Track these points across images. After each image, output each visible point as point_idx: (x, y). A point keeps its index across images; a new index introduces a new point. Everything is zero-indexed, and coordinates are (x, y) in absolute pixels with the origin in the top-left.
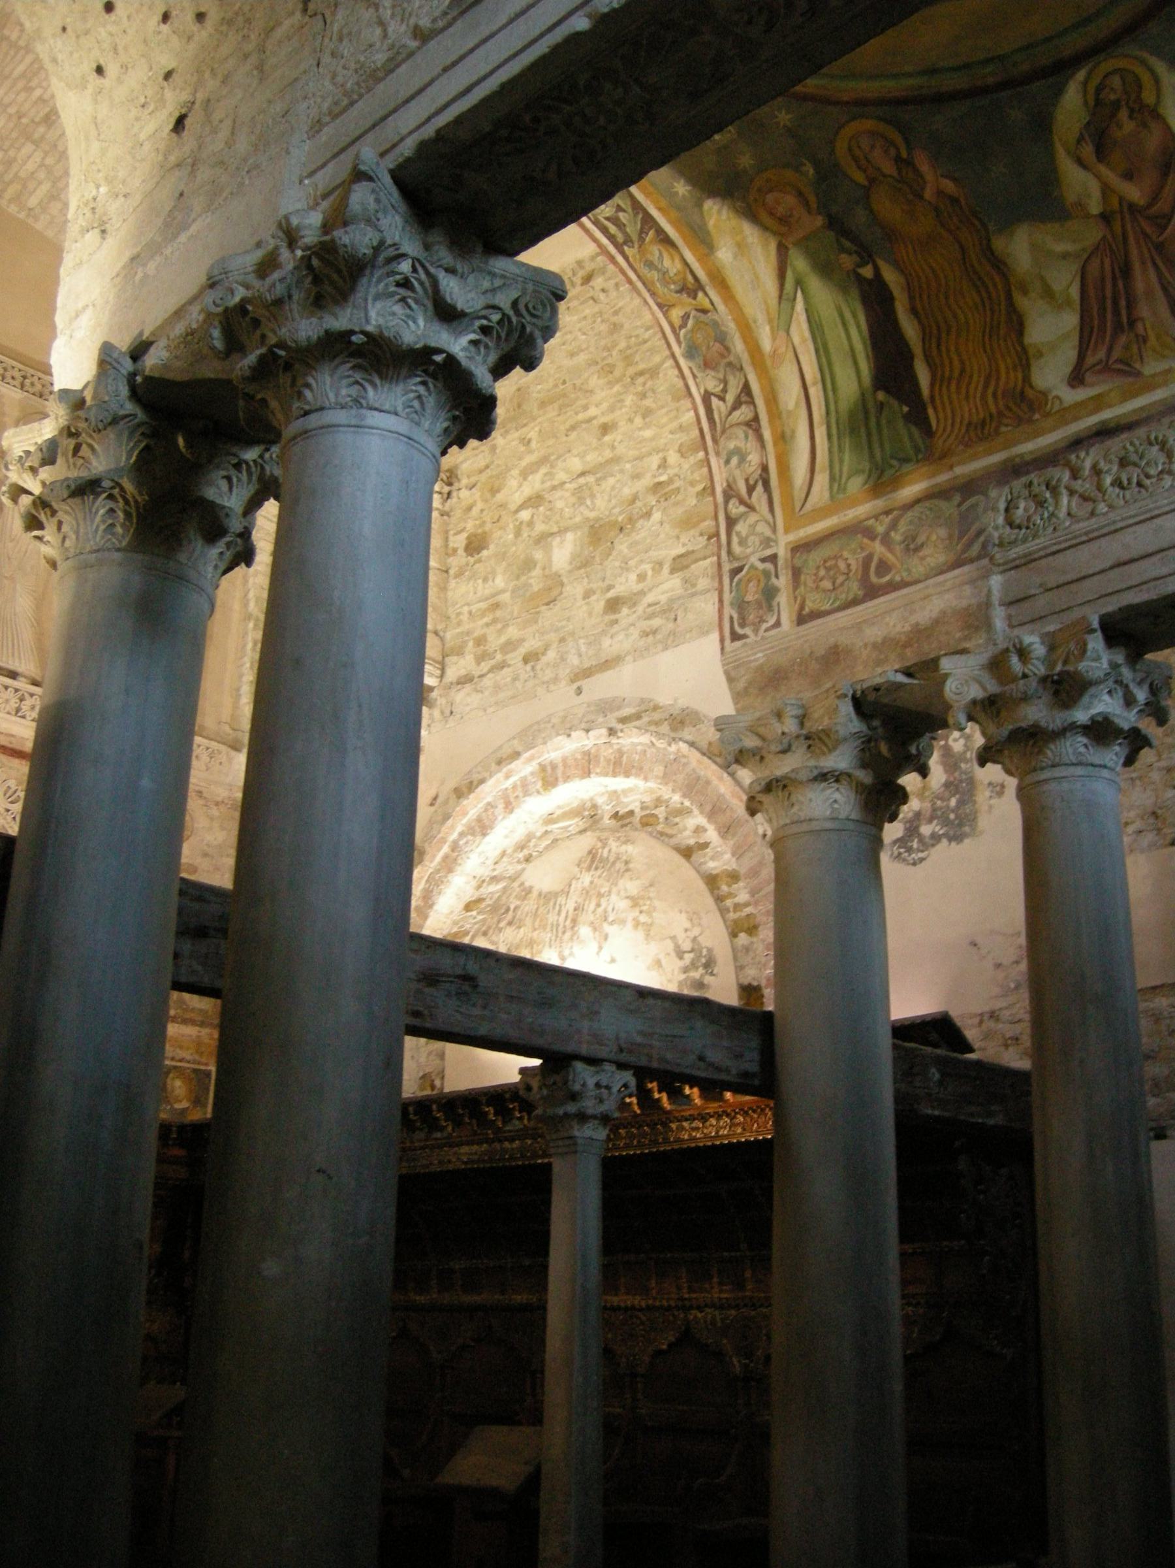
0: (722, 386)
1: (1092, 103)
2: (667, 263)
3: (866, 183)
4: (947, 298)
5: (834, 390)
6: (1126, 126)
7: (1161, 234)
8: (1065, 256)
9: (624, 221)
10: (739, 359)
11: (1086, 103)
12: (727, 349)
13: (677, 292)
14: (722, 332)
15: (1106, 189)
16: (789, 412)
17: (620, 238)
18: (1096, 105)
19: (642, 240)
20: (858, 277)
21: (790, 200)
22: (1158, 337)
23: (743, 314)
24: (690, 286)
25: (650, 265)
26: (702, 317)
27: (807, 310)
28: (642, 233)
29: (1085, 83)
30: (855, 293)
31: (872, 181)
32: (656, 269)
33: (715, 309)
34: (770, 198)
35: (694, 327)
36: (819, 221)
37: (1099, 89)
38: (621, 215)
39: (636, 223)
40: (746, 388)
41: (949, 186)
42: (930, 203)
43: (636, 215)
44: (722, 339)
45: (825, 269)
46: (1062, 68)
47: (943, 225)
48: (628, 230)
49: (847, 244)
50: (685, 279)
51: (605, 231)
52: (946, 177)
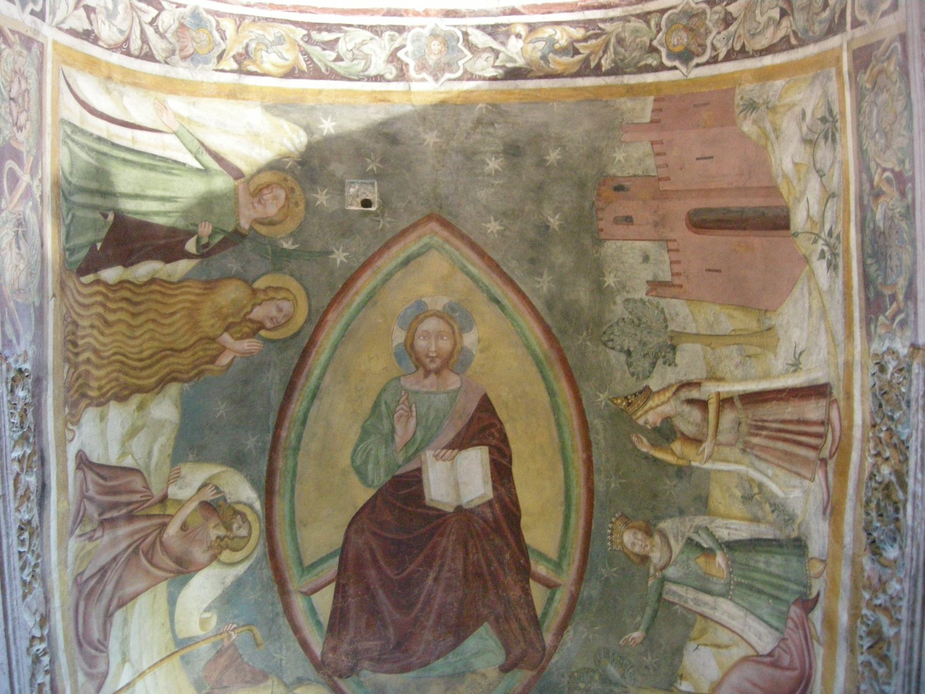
0: (161, 29)
1: (239, 507)
2: (274, 58)
3: (257, 285)
4: (154, 321)
5: (125, 161)
6: (215, 532)
7: (143, 552)
8: (150, 454)
9: (327, 52)
10: (174, 65)
11: (239, 502)
12: (184, 58)
13: (247, 46)
14: (199, 62)
15: (180, 504)
16: (122, 95)
17: (315, 35)
18: (233, 509)
19: (305, 53)
20: (190, 234)
21: (272, 210)
22: (89, 553)
23: (204, 96)
24: (246, 62)
25: (280, 41)
26: (217, 52)
27: (184, 164)
28: (309, 60)
29: (251, 507)
30: (181, 224)
31: (254, 292)
32: (273, 44)
33: (216, 70)
34: (282, 194)
35: (213, 36)
36: (245, 225)
37: (243, 516)
38: (333, 55)
39: (320, 60)
40: (149, 57)
41: (225, 360)
42: (221, 335)
43: (327, 67)
44: (192, 58)
45: (207, 203)
46: (268, 494)
47: (201, 339)
48: (318, 49)
49: (218, 238)
50: (254, 62)
51: (329, 28)
52: (233, 360)
